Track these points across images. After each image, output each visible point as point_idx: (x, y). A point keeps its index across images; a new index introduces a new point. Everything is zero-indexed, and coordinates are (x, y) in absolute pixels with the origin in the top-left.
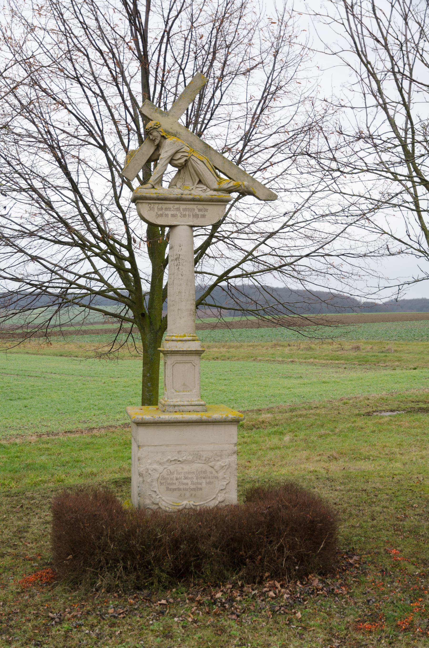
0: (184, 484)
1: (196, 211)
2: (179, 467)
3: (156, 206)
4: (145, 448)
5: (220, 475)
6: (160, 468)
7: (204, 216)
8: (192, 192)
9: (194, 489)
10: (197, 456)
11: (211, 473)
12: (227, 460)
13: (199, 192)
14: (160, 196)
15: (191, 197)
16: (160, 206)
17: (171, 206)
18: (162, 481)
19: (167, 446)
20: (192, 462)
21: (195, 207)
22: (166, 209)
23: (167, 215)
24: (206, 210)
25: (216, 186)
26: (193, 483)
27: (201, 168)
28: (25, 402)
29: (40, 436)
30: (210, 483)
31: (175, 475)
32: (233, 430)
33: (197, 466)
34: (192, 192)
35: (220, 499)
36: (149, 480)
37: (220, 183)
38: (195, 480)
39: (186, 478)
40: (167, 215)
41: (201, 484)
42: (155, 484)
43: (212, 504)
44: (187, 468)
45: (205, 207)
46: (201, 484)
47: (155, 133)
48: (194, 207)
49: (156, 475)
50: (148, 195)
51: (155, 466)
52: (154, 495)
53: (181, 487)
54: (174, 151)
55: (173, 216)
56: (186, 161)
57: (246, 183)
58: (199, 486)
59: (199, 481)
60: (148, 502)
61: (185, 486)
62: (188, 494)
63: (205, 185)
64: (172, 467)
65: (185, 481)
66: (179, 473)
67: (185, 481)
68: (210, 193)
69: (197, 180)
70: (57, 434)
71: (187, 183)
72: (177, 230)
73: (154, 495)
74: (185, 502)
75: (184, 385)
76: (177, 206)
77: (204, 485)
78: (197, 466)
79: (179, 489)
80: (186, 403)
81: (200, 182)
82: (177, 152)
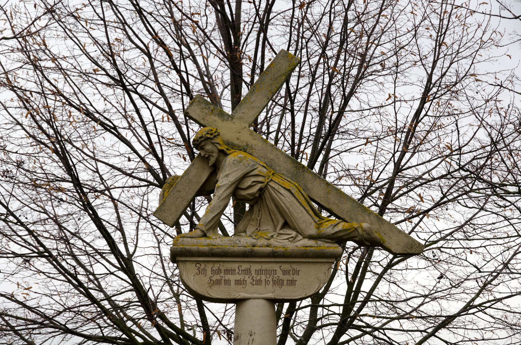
1: (280, 274)
3: (209, 267)
7: (292, 283)
8: (272, 241)
13: (283, 241)
14: (216, 250)
15: (269, 249)
16: (216, 266)
17: (235, 266)
21: (278, 269)
22: (227, 271)
23: (227, 282)
24: (297, 272)
25: (313, 231)
27: (287, 200)
34: (272, 241)
37: (319, 226)
40: (227, 282)
45: (295, 266)
47: (209, 147)
48: (276, 267)
50: (194, 248)
54: (238, 174)
55: (238, 282)
56: (261, 190)
57: (365, 225)
63: (294, 229)
68: (302, 243)
69: (281, 222)
71: (263, 228)
72: (248, 306)
76: (245, 266)
81: (286, 225)
82: (245, 176)
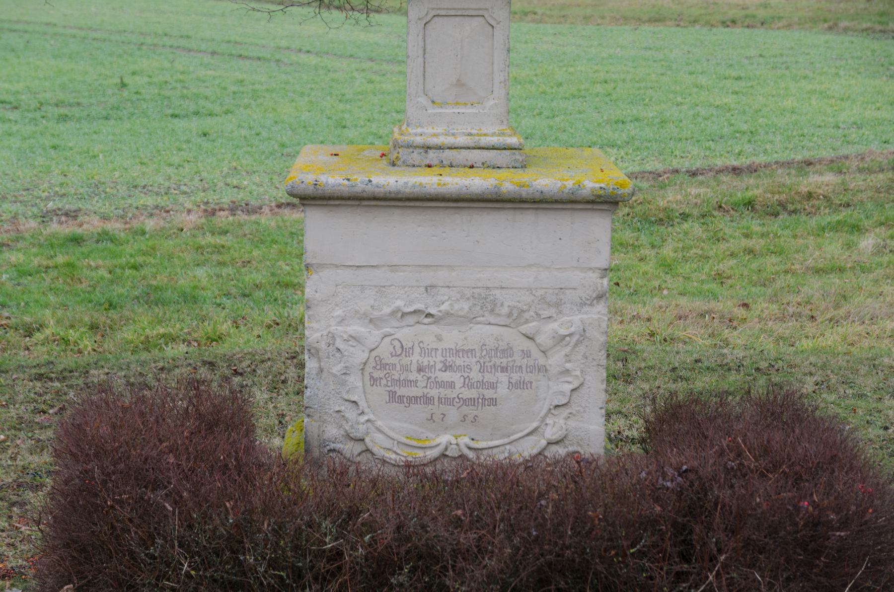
0: (441, 384)
2: (427, 333)
4: (326, 273)
5: (555, 360)
6: (373, 336)
9: (472, 402)
10: (485, 303)
11: (527, 354)
12: (576, 318)
18: (377, 371)
19: (394, 268)
20: (470, 319)
26: (468, 383)
30: (520, 385)
31: (415, 358)
32: (599, 228)
33: (482, 333)
35: (551, 433)
36: (337, 369)
38: (475, 375)
39: (447, 368)
41: (493, 386)
42: (355, 380)
43: (528, 448)
44: (452, 336)
46: (493, 386)
49: (359, 355)
51: (356, 328)
52: (351, 414)
53: (434, 392)
58: (489, 393)
59: (489, 377)
60: (332, 431)
61: (444, 392)
62: (453, 414)
64: (406, 334)
65: (446, 376)
66: (426, 352)
67: (446, 376)
73: (351, 414)
74: (444, 439)
75: (459, 84)
78: (482, 333)
79: (428, 400)
80: (461, 140)
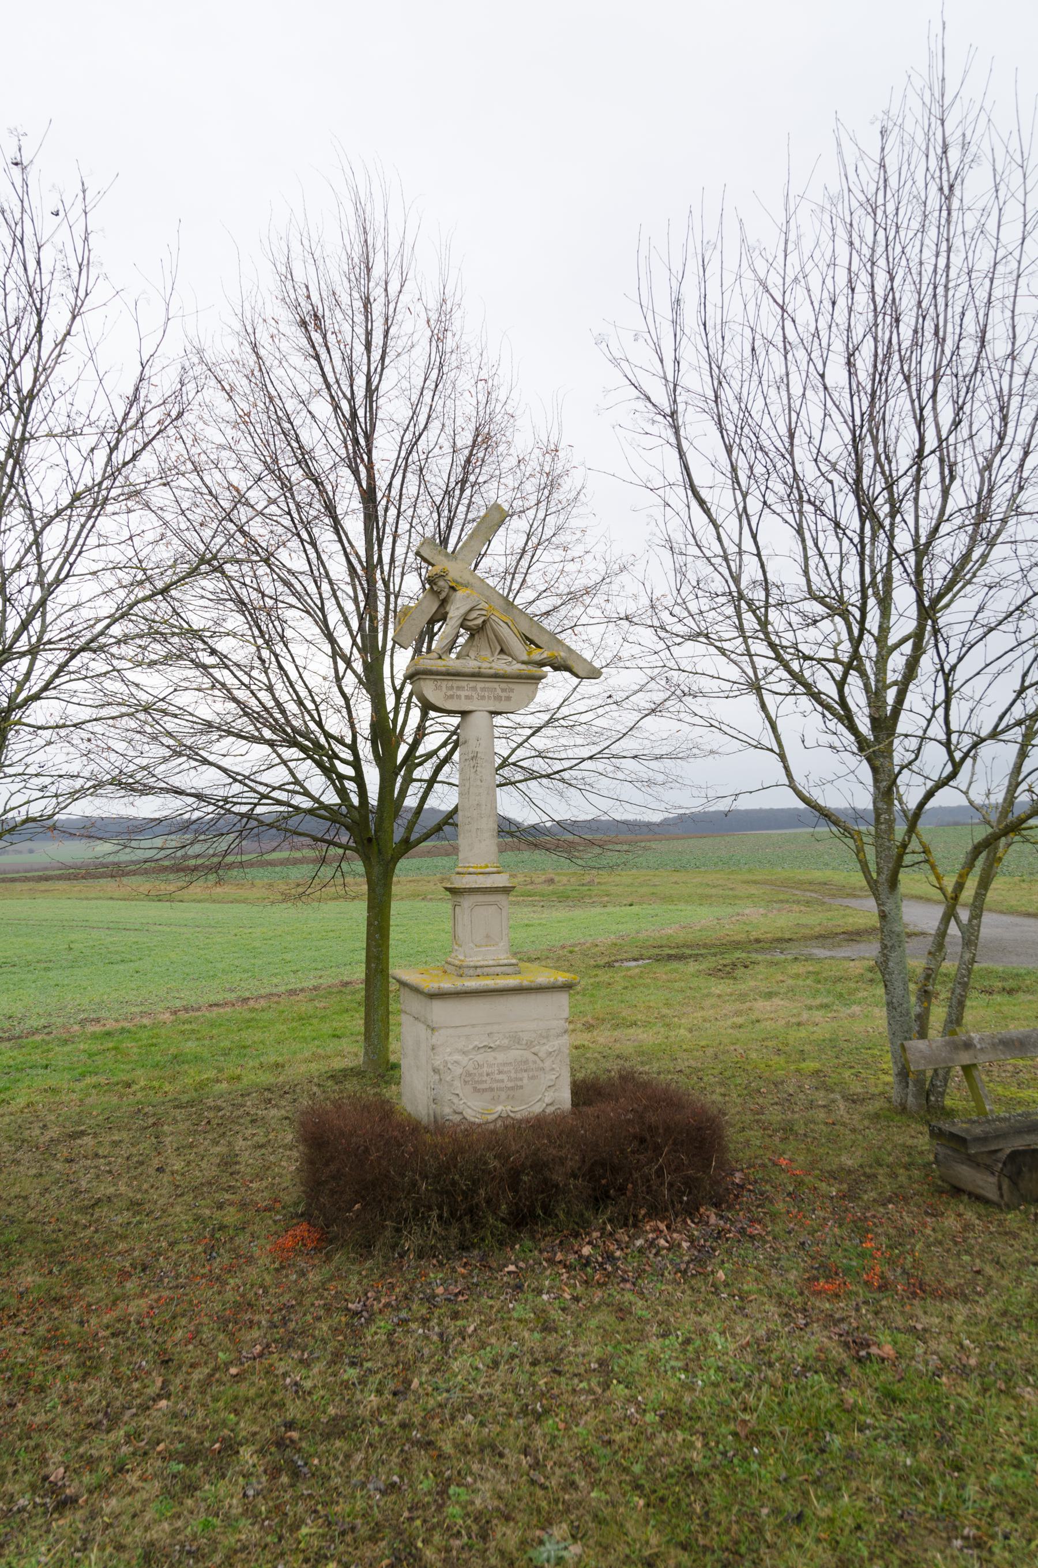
0: (498, 1081)
1: (499, 691)
2: (490, 1056)
3: (444, 684)
4: (442, 1031)
5: (547, 1064)
6: (464, 1060)
7: (508, 699)
8: (493, 665)
9: (512, 1088)
10: (515, 1039)
11: (535, 1062)
12: (556, 1043)
13: (502, 665)
14: (451, 670)
15: (492, 671)
16: (450, 683)
17: (464, 684)
18: (468, 1078)
19: (473, 1026)
20: (508, 1048)
21: (497, 686)
22: (458, 688)
23: (459, 697)
24: (512, 690)
25: (525, 658)
26: (510, 1080)
27: (505, 632)
28: (135, 965)
29: (175, 1013)
30: (533, 1078)
31: (485, 1069)
32: (563, 999)
33: (515, 1054)
34: (493, 665)
35: (547, 1100)
36: (448, 1078)
37: (529, 653)
38: (513, 1075)
39: (500, 1072)
40: (459, 697)
41: (521, 1079)
42: (457, 1083)
43: (537, 1109)
44: (501, 1057)
45: (511, 686)
46: (521, 1079)
47: (441, 583)
48: (496, 685)
49: (458, 1070)
50: (434, 668)
51: (457, 1057)
52: (456, 1100)
53: (495, 1085)
54: (468, 607)
55: (467, 697)
56: (484, 622)
57: (562, 654)
58: (519, 1083)
59: (519, 1075)
60: (447, 1110)
61: (499, 1085)
62: (503, 1095)
63: (510, 655)
64: (479, 1058)
65: (500, 1077)
66: (490, 1066)
67: (500, 1077)
68: (516, 667)
69: (499, 649)
70: (199, 1009)
71: (483, 653)
72: (472, 718)
73: (456, 1100)
74: (500, 1108)
75: (488, 936)
76: (472, 684)
77: (525, 1081)
78: (515, 1054)
79: (492, 1089)
80: (491, 963)
81: (502, 651)
82: (471, 610)
